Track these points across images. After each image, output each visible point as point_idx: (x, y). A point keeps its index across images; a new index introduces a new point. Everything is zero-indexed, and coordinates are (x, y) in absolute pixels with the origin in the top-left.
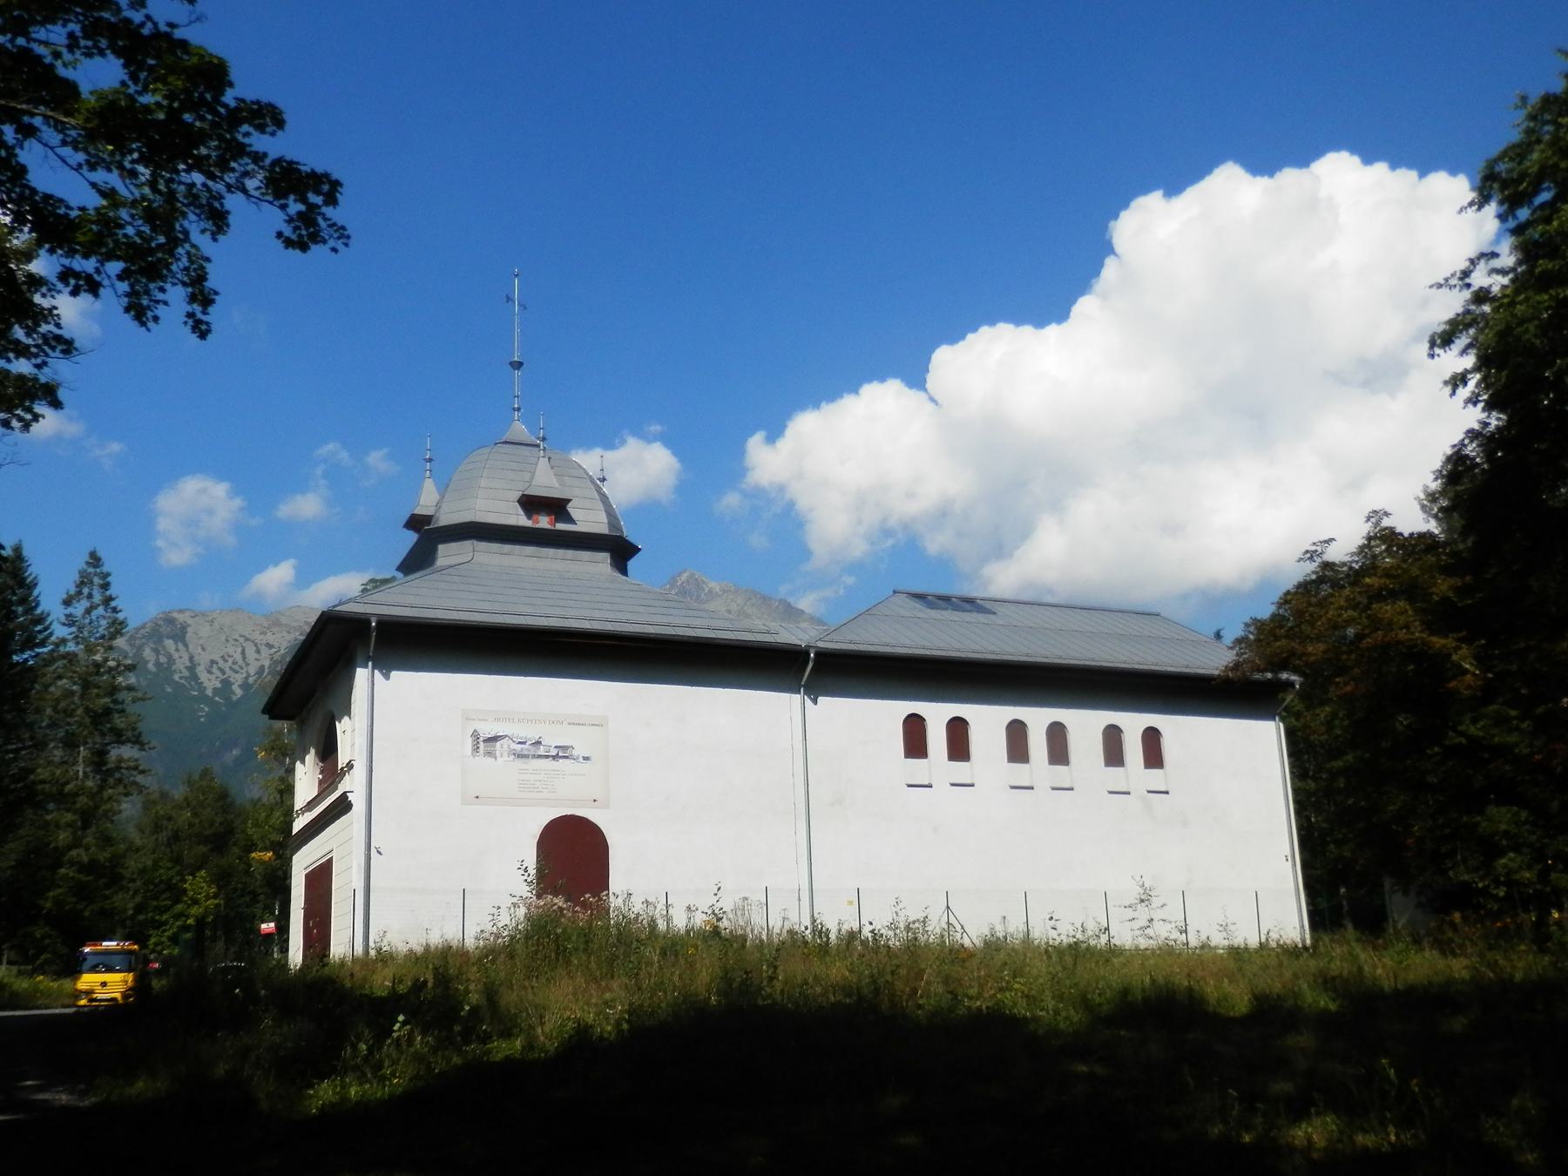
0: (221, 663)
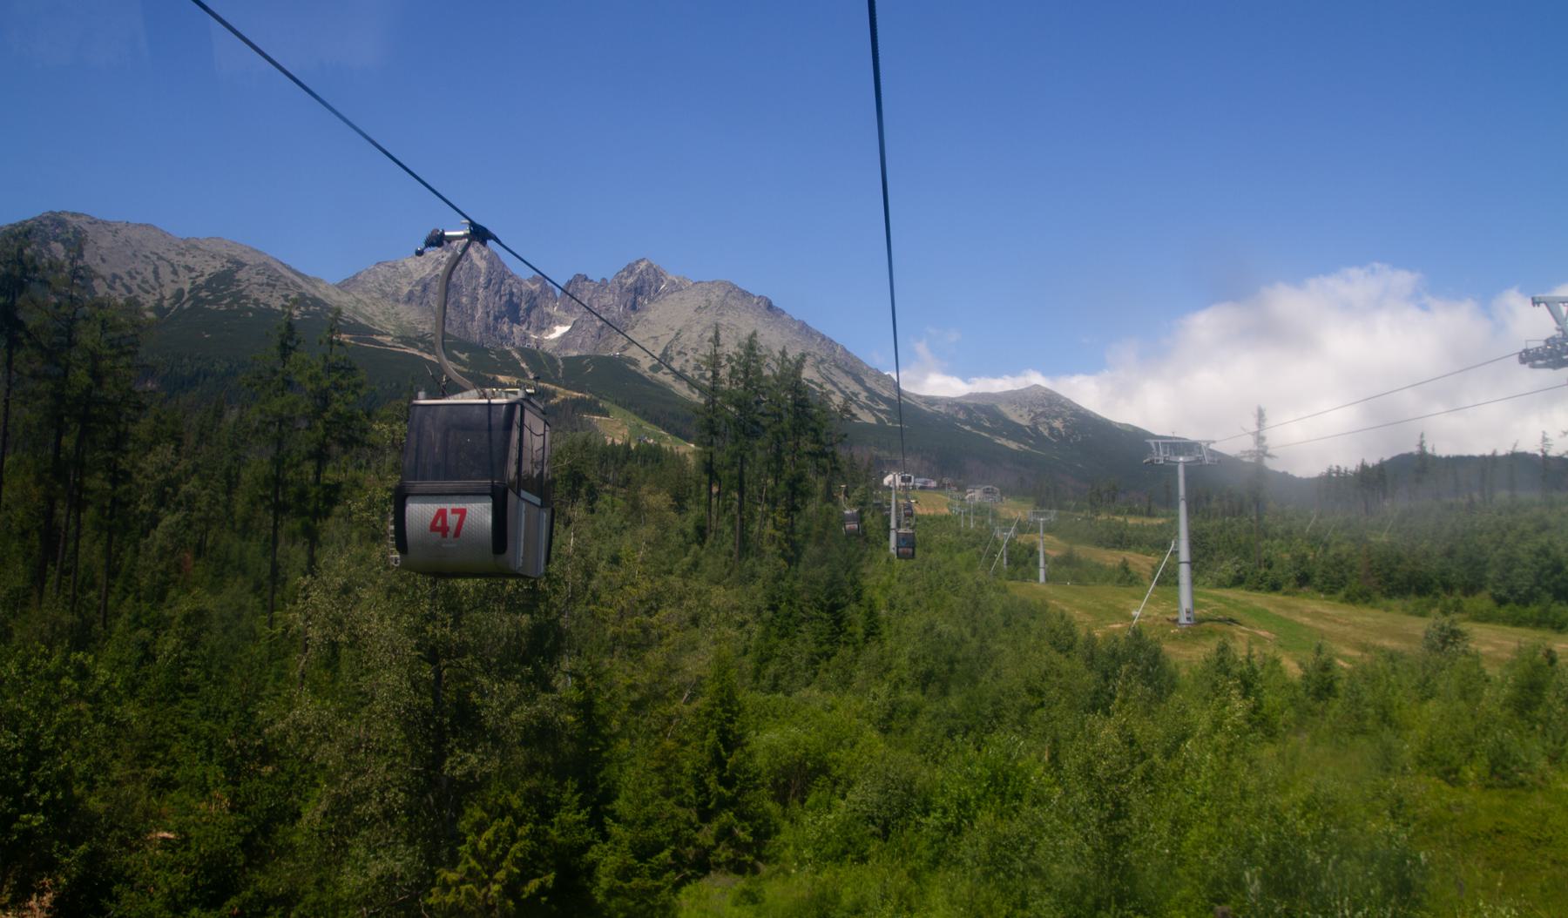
0: (127, 279)
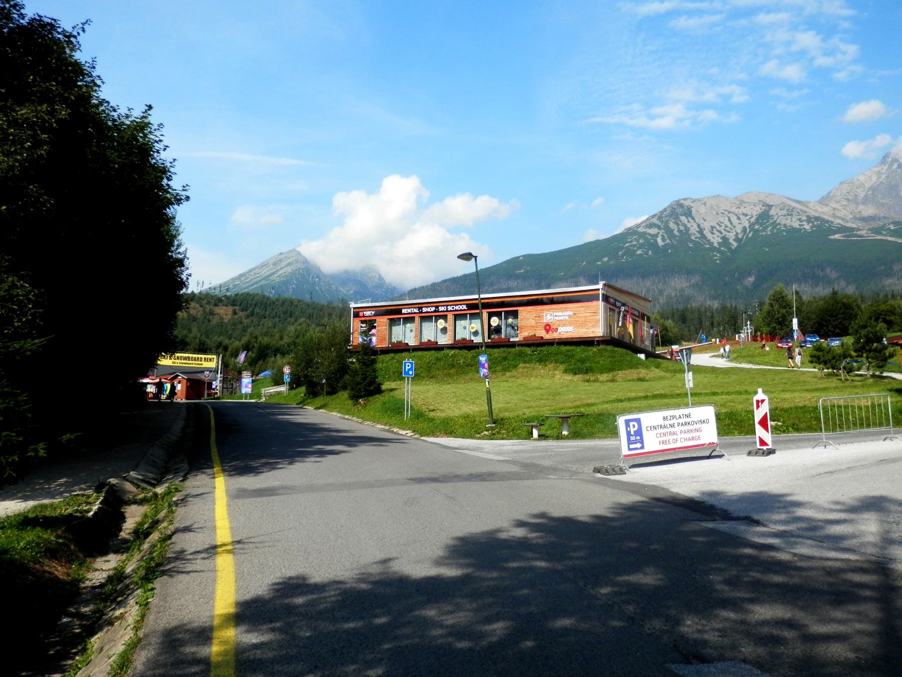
0: (718, 228)
